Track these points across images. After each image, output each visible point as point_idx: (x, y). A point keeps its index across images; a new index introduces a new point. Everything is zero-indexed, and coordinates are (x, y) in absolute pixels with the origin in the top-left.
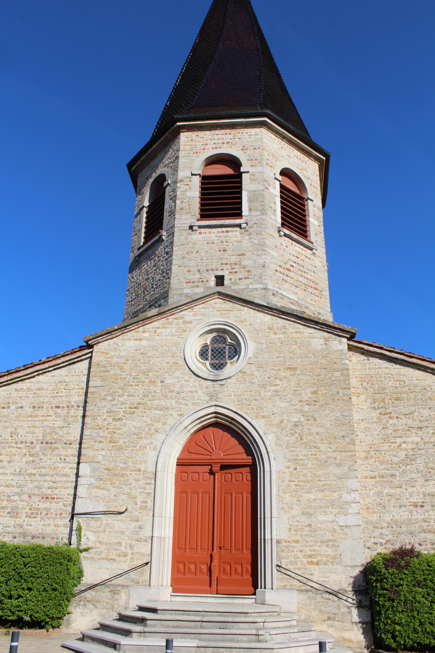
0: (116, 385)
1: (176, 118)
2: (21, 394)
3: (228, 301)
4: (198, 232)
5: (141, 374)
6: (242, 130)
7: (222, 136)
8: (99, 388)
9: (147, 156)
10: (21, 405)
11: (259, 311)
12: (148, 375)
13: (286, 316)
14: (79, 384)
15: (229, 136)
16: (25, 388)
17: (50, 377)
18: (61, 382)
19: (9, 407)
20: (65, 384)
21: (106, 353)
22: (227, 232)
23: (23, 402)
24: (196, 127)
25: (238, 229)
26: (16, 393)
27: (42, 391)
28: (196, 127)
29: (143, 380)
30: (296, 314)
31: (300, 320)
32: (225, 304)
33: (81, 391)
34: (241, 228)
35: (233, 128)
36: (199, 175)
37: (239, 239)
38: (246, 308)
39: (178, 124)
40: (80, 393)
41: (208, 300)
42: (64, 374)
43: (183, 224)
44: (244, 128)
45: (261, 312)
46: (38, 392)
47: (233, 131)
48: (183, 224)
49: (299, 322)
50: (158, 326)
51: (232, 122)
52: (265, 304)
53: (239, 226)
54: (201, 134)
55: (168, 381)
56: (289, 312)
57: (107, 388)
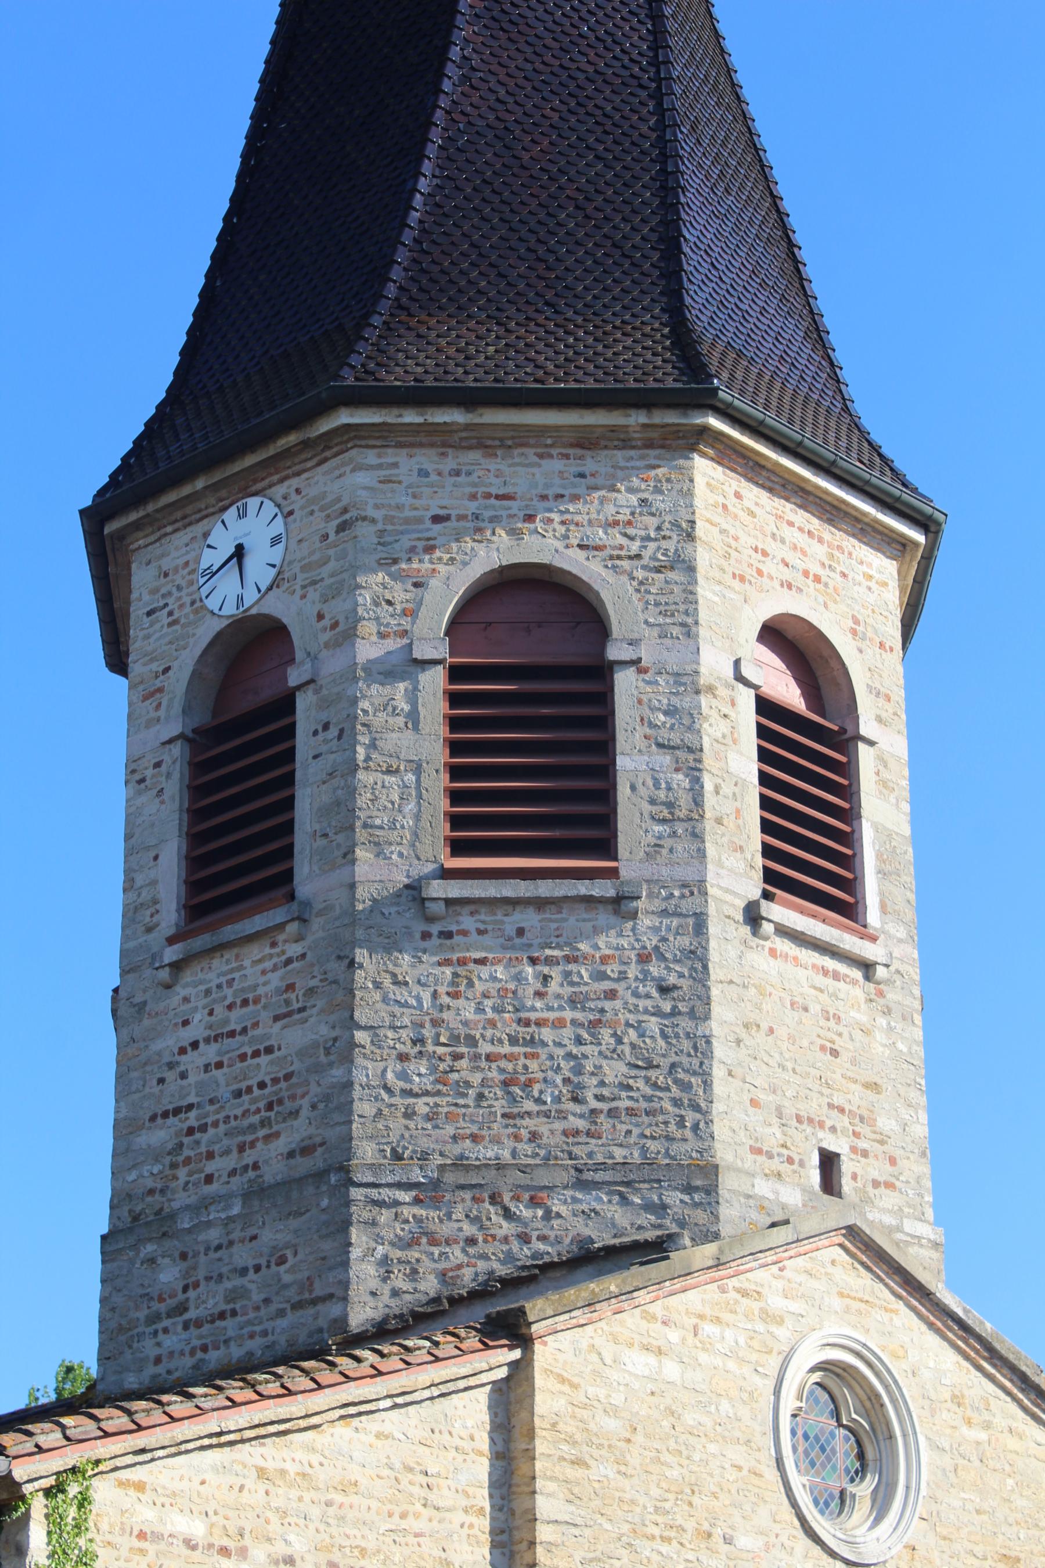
0: (607, 1526)
1: (722, 401)
2: (282, 1496)
3: (862, 1264)
4: (768, 944)
5: (671, 1497)
6: (850, 543)
7: (802, 540)
8: (564, 1528)
9: (468, 427)
10: (288, 1551)
11: (931, 1326)
12: (690, 1504)
13: (994, 1366)
14: (471, 1490)
15: (819, 551)
16: (292, 1468)
17: (371, 1439)
18: (410, 1470)
19: (243, 1553)
20: (424, 1480)
21: (575, 1386)
22: (836, 976)
23: (291, 1538)
24: (744, 457)
25: (857, 974)
26: (262, 1487)
27: (354, 1499)
28: (744, 457)
29: (680, 1521)
30: (1024, 1368)
31: (1022, 1390)
32: (853, 1273)
33: (473, 1519)
34: (868, 978)
35: (830, 521)
36: (756, 687)
37: (863, 1019)
38: (900, 1305)
39: (715, 422)
40: (475, 1531)
41: (820, 1244)
42: (422, 1434)
43: (727, 891)
44: (854, 536)
45: (938, 1331)
46: (339, 1498)
47: (828, 532)
48: (727, 891)
49: (1020, 1396)
50: (699, 1308)
51: (844, 502)
52: (960, 1313)
53: (867, 967)
54: (754, 495)
55: (743, 1541)
56: (1011, 1357)
57: (587, 1532)
